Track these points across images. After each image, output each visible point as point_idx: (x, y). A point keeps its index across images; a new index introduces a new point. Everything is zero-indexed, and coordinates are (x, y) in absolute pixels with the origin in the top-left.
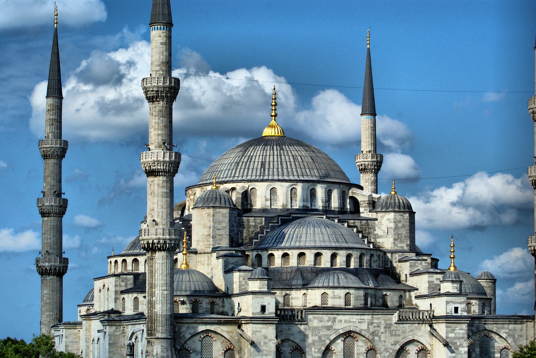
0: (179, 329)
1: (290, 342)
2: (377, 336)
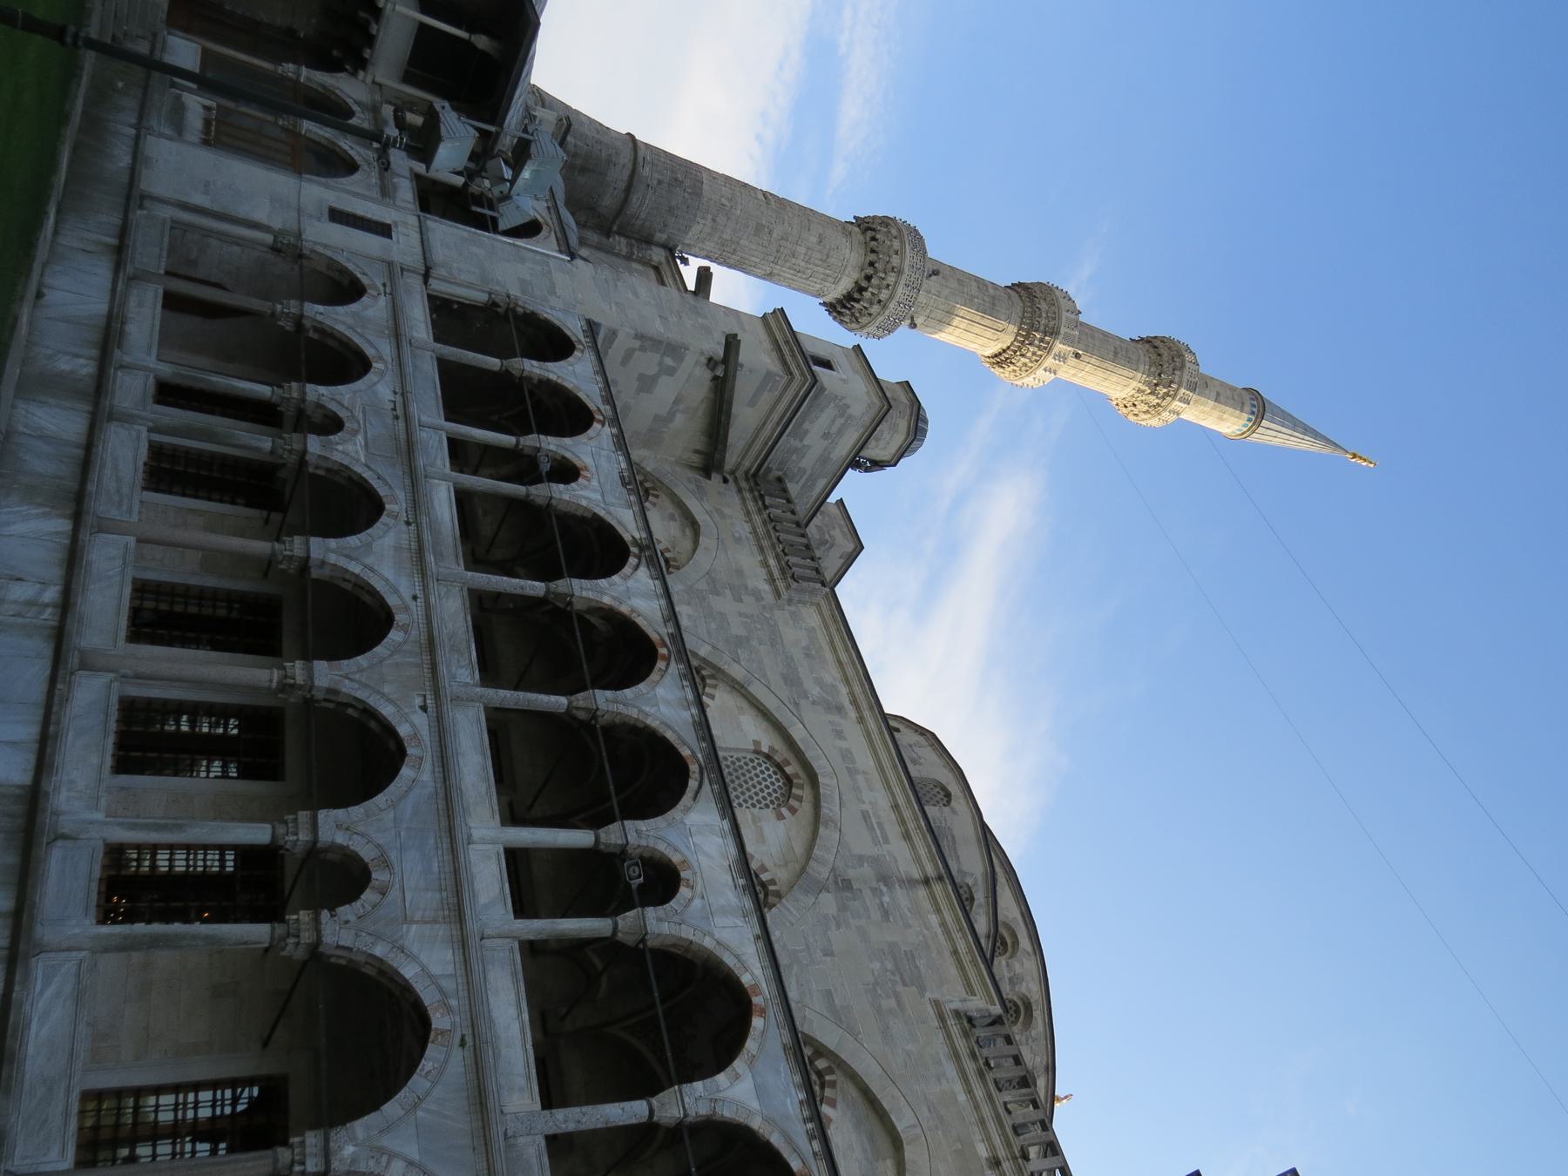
1: (688, 545)
2: (843, 908)
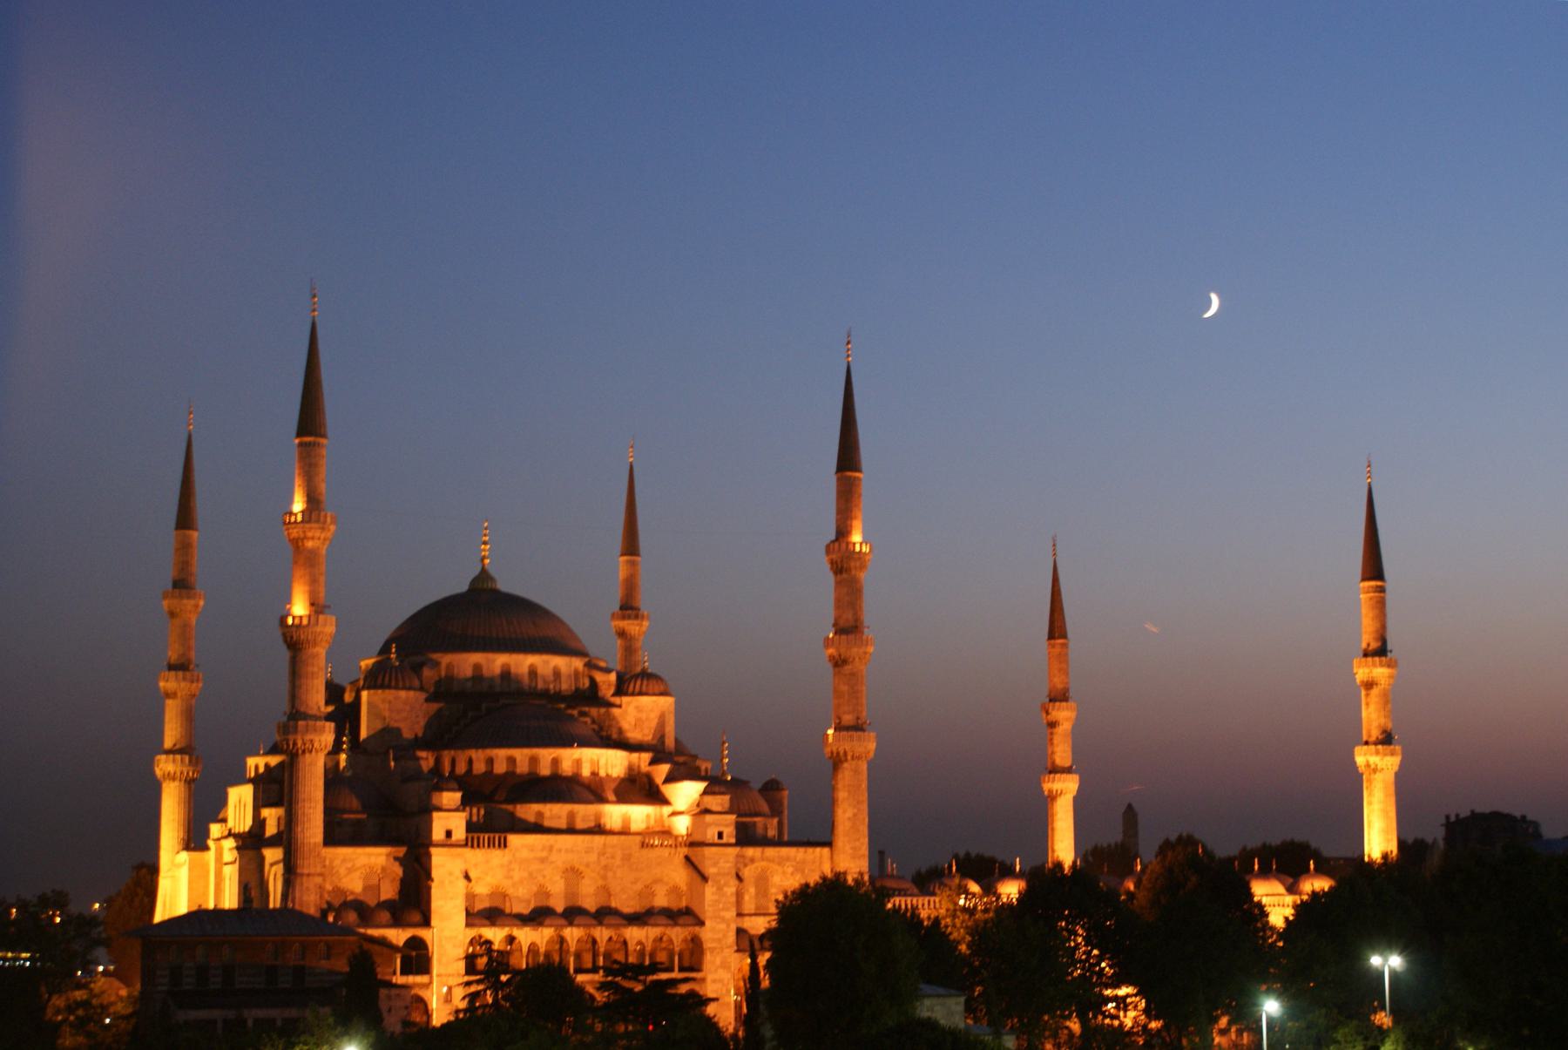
0: (332, 861)
